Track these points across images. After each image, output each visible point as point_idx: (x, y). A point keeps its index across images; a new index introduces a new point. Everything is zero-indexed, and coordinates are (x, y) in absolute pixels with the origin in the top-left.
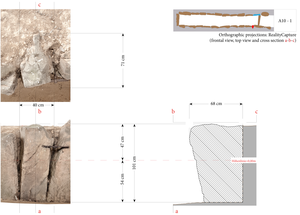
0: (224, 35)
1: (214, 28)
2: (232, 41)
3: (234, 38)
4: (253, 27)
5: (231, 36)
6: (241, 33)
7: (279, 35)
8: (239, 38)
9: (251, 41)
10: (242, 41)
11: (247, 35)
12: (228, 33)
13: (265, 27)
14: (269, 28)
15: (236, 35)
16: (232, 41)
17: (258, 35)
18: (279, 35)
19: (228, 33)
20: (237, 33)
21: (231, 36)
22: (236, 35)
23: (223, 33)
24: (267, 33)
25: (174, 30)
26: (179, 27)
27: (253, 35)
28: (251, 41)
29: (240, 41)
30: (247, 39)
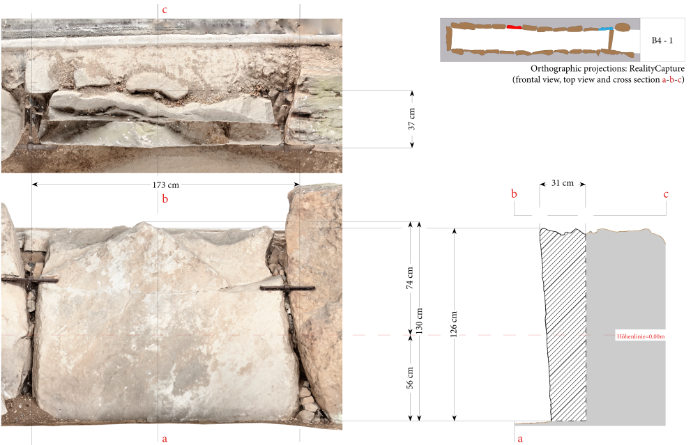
2: (557, 80)
3: (561, 75)
4: (598, 52)
5: (555, 70)
6: (574, 64)
8: (571, 75)
9: (596, 81)
10: (577, 80)
11: (587, 69)
12: (549, 65)
15: (565, 70)
16: (557, 80)
19: (549, 65)
20: (567, 64)
21: (555, 70)
22: (565, 70)
27: (598, 69)
28: (596, 81)
29: (572, 81)
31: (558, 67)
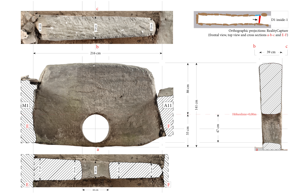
0: (233, 31)
1: (225, 25)
3: (240, 33)
5: (238, 31)
6: (245, 29)
7: (275, 31)
8: (244, 33)
11: (250, 31)
12: (236, 29)
13: (264, 25)
14: (267, 25)
15: (242, 31)
16: (239, 35)
17: (259, 31)
18: (275, 31)
19: (236, 29)
20: (243, 29)
21: (238, 31)
22: (242, 31)
23: (232, 29)
24: (266, 29)
25: (195, 27)
26: (198, 24)
27: (255, 31)
30: (250, 34)
31: (239, 30)
